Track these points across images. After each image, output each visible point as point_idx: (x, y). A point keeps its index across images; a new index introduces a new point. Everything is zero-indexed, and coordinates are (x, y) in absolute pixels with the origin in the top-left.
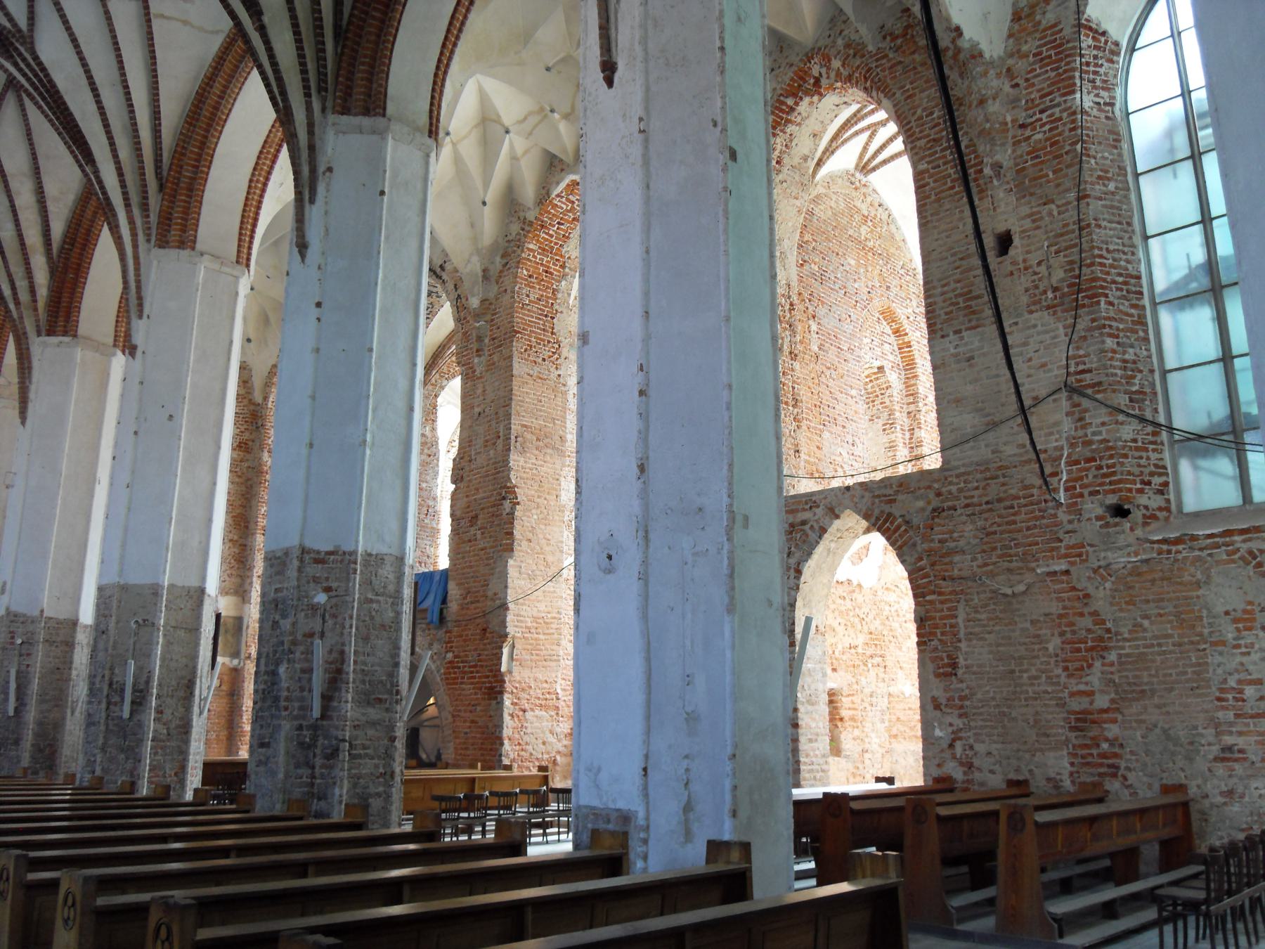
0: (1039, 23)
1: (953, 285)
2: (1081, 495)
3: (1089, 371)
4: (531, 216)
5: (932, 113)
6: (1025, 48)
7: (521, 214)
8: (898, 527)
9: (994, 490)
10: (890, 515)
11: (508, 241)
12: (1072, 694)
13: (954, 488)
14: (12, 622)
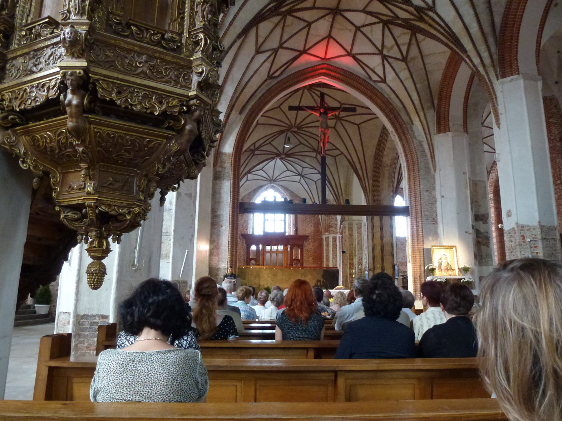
14: (521, 230)
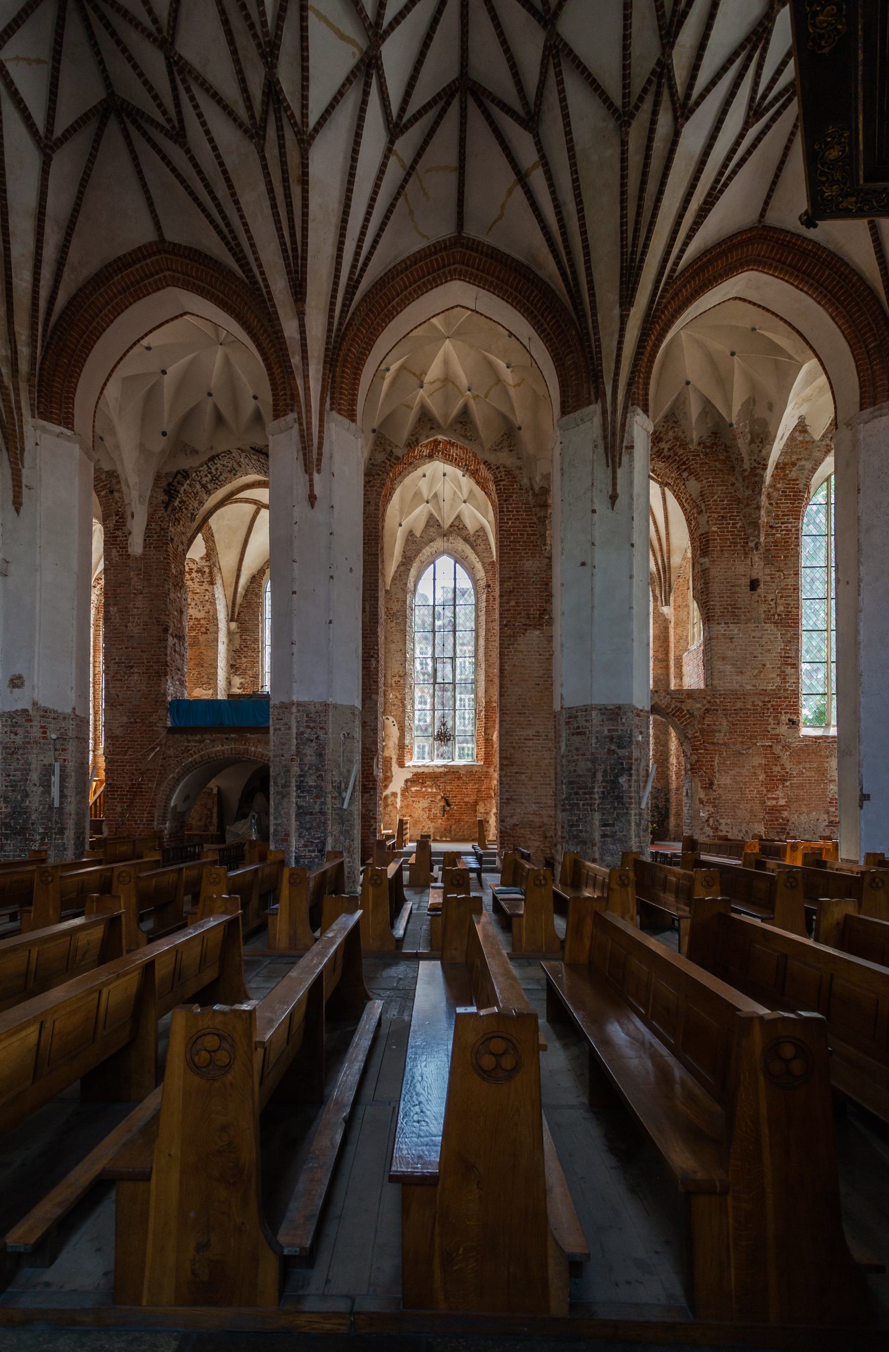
0: (787, 475)
1: (726, 598)
2: (781, 713)
3: (790, 657)
4: (399, 452)
5: (723, 501)
6: (779, 486)
7: (388, 448)
8: (685, 715)
9: (739, 705)
10: (680, 708)
11: (372, 464)
12: (768, 799)
13: (718, 701)
